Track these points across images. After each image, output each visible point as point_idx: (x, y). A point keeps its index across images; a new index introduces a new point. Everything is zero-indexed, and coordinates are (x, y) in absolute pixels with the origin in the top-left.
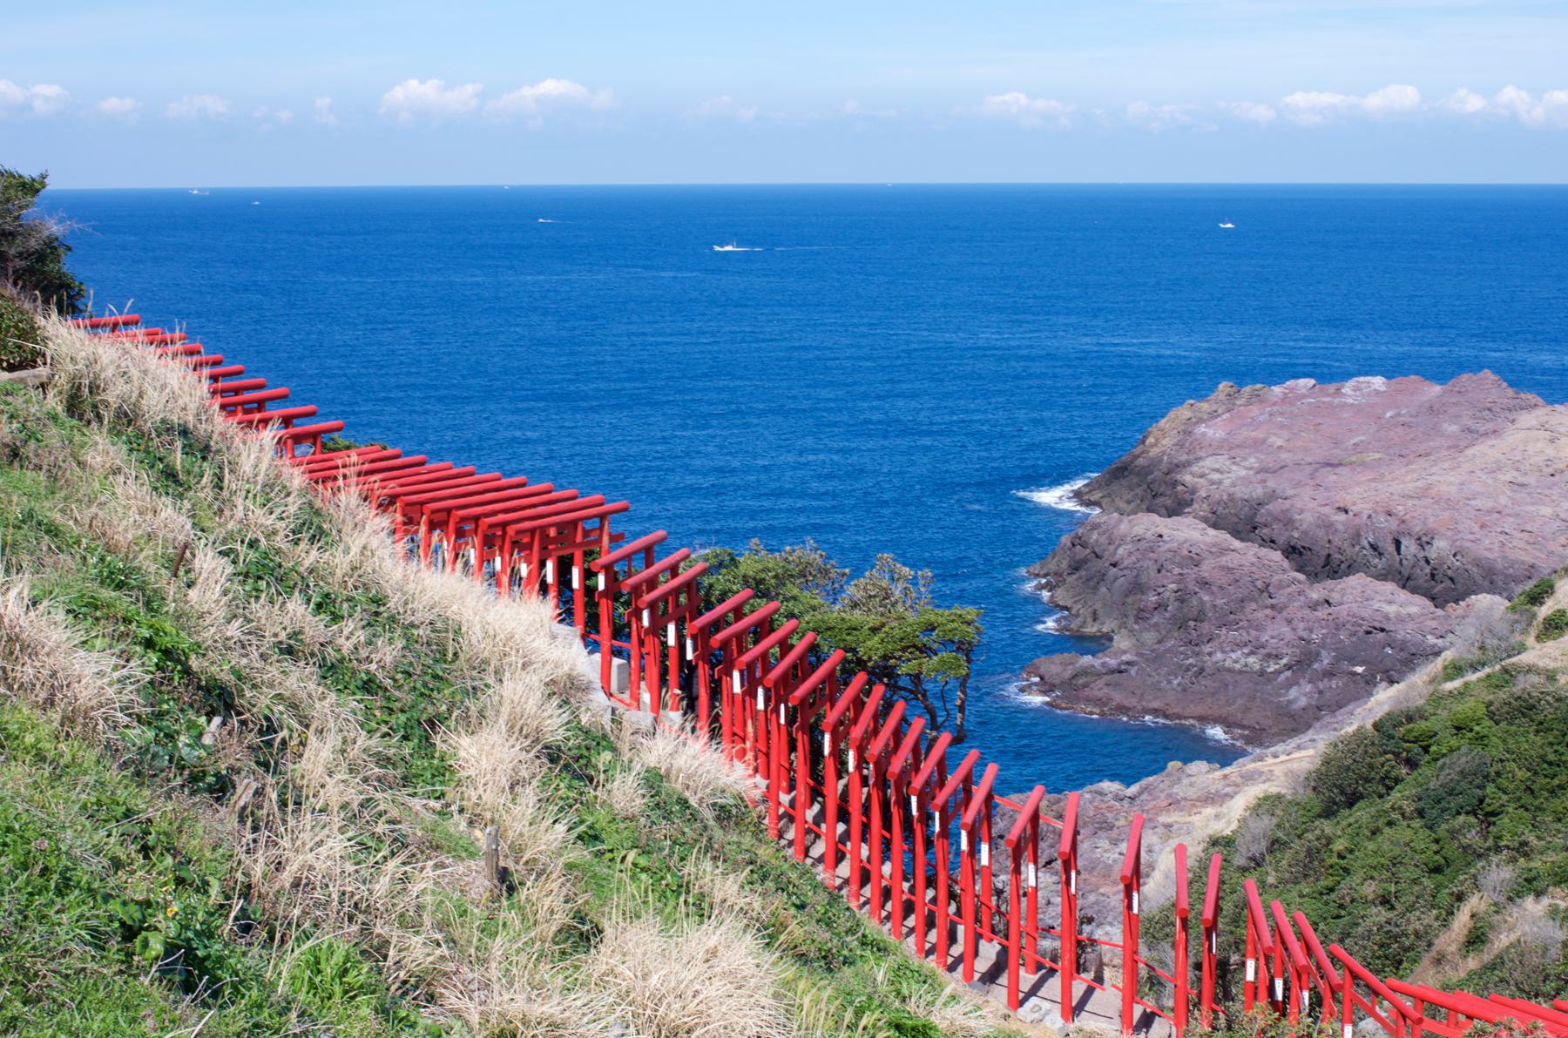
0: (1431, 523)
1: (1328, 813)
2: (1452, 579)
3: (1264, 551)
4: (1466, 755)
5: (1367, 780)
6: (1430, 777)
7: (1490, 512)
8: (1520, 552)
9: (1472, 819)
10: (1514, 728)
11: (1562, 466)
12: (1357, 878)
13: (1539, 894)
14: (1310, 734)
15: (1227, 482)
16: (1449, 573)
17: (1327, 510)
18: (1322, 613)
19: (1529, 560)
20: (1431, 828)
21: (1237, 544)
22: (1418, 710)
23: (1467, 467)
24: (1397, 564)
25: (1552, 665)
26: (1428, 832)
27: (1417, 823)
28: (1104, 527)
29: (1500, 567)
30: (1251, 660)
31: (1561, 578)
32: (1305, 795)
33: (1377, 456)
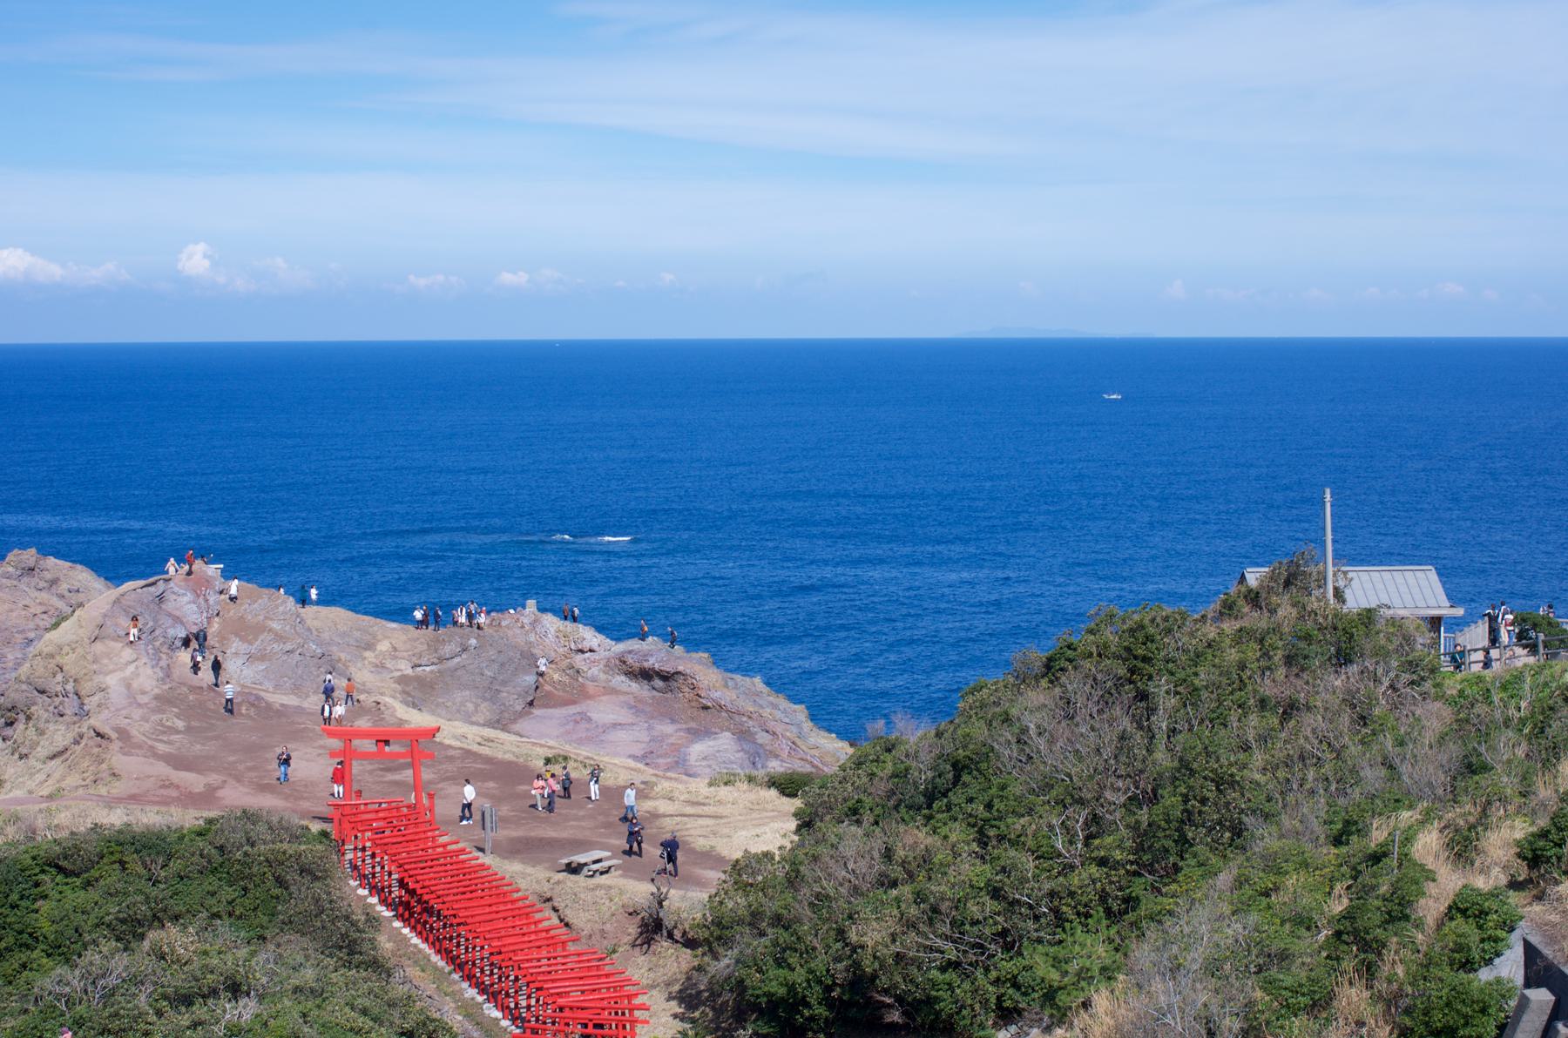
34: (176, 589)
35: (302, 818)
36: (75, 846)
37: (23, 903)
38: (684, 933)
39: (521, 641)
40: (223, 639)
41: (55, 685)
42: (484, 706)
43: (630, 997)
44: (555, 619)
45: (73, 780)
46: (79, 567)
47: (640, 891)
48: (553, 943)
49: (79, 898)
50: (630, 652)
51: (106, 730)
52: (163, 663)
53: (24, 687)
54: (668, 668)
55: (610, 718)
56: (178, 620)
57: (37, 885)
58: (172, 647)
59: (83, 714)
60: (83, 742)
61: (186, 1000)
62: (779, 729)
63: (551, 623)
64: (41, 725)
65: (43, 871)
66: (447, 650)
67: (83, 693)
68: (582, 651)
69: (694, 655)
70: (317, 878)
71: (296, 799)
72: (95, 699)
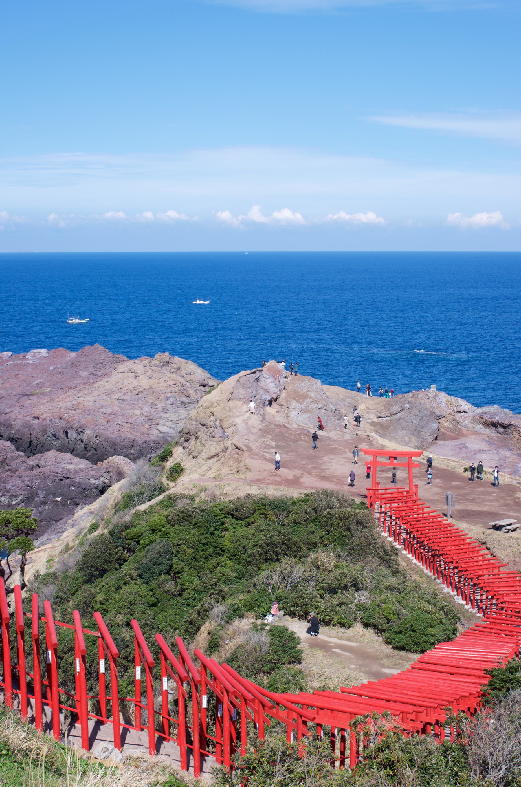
1: (88, 581)
2: (95, 449)
4: (160, 544)
5: (110, 562)
6: (142, 557)
7: (110, 414)
8: (128, 434)
9: (167, 577)
10: (182, 528)
11: (142, 390)
12: (112, 614)
13: (241, 617)
14: (46, 537)
16: (94, 446)
17: (28, 418)
18: (36, 472)
20: (147, 583)
22: (130, 522)
24: (67, 444)
25: (191, 493)
27: (139, 581)
29: (118, 441)
32: (72, 572)
33: (49, 389)
34: (265, 375)
36: (242, 505)
37: (216, 532)
39: (428, 406)
41: (210, 422)
42: (414, 439)
45: (225, 470)
46: (190, 362)
48: (492, 566)
50: (485, 413)
51: (240, 445)
52: (262, 412)
53: (194, 422)
54: (506, 422)
56: (266, 391)
57: (223, 523)
58: (264, 405)
59: (224, 437)
60: (228, 452)
61: (333, 591)
63: (443, 397)
64: (203, 442)
65: (225, 517)
66: (395, 409)
67: (224, 426)
68: (459, 412)
70: (365, 527)
71: (341, 484)
72: (231, 430)
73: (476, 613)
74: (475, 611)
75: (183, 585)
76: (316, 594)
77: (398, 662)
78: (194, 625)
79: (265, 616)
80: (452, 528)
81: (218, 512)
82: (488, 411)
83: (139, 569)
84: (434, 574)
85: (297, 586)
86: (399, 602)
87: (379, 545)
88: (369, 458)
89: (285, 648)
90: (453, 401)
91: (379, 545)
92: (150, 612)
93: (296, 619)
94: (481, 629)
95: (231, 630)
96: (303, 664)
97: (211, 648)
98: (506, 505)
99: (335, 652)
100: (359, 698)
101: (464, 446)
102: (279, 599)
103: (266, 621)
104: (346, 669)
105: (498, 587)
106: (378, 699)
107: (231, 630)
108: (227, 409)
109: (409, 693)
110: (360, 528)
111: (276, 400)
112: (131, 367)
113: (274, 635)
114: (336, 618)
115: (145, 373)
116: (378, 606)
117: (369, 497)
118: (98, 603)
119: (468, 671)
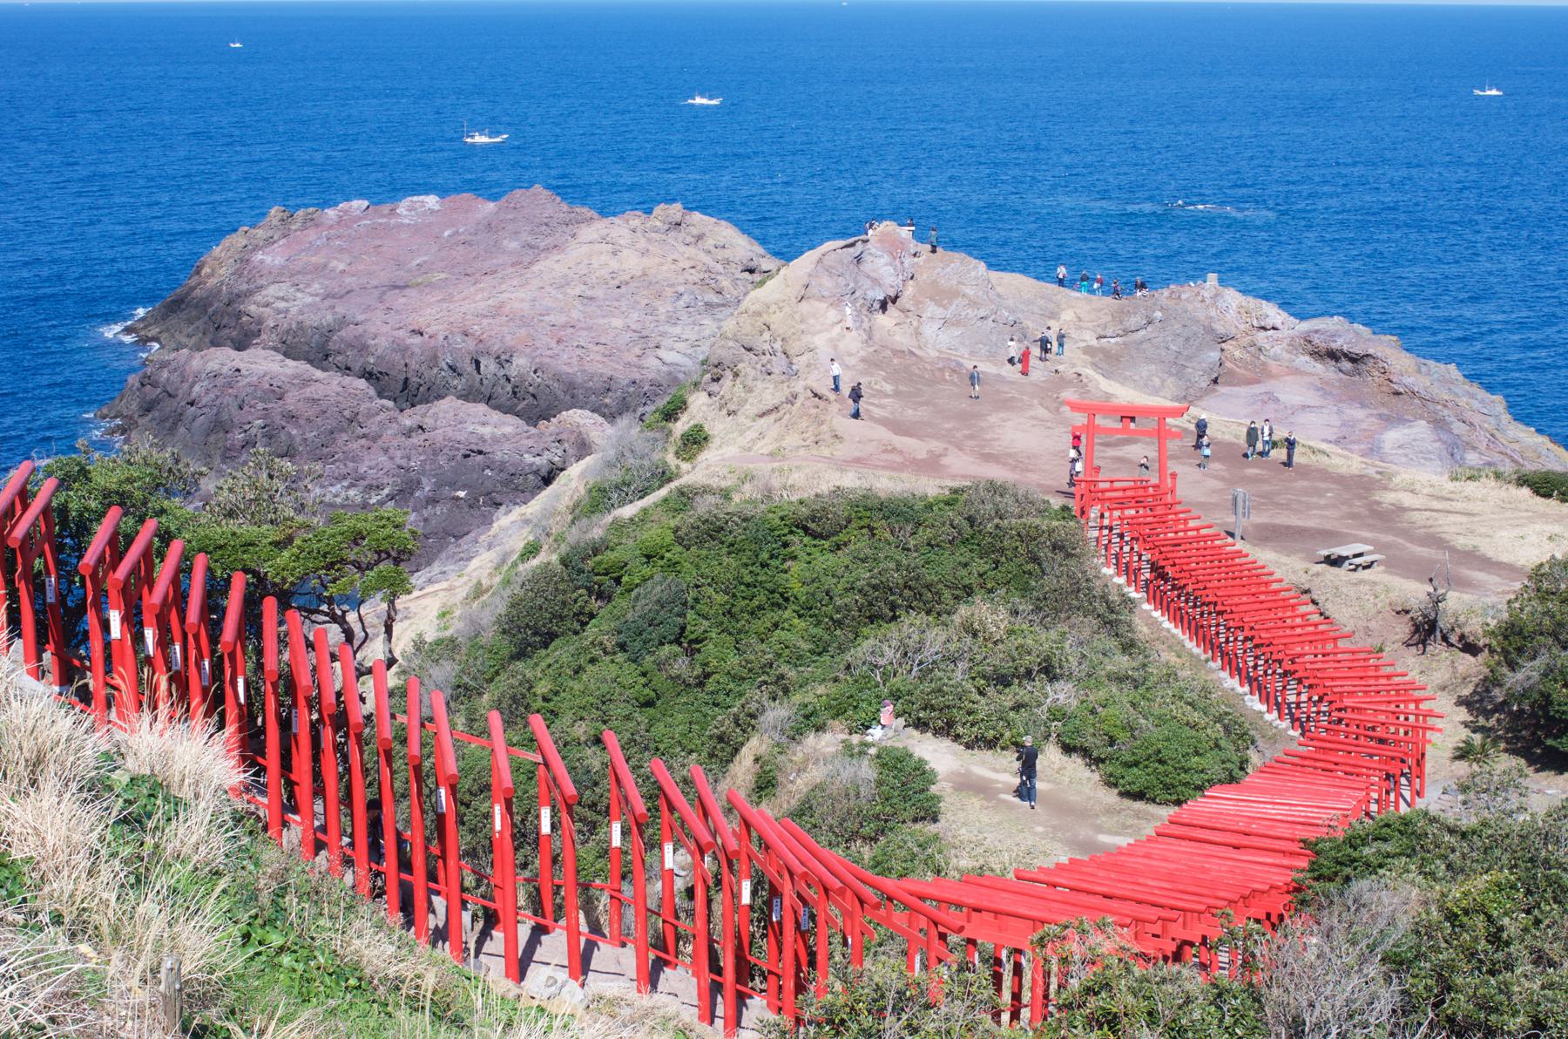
0: (510, 341)
1: (520, 655)
2: (534, 396)
3: (348, 380)
5: (562, 618)
7: (564, 327)
8: (598, 366)
9: (676, 648)
10: (704, 552)
11: (627, 277)
12: (567, 719)
13: (820, 728)
14: (436, 568)
15: (294, 310)
16: (531, 389)
17: (401, 333)
18: (417, 439)
19: (610, 373)
20: (634, 661)
21: (319, 374)
23: (536, 283)
24: (477, 384)
25: (724, 484)
26: (634, 666)
27: (620, 657)
28: (174, 365)
29: (579, 379)
30: (352, 493)
31: (691, 392)
32: (489, 636)
33: (443, 276)
35: (1047, 492)
37: (773, 563)
38: (1462, 637)
39: (1201, 315)
40: (917, 303)
41: (762, 343)
42: (1170, 381)
43: (1417, 701)
44: (1238, 294)
45: (792, 440)
46: (723, 223)
47: (1415, 592)
48: (1324, 638)
49: (826, 560)
50: (1316, 332)
52: (866, 325)
53: (731, 344)
54: (1358, 350)
55: (1297, 399)
56: (876, 282)
57: (785, 545)
58: (870, 310)
59: (791, 374)
60: (798, 404)
61: (1003, 681)
62: (1477, 419)
63: (1232, 298)
64: (749, 382)
65: (791, 532)
66: (1134, 321)
67: (791, 352)
68: (1264, 328)
69: (1383, 337)
70: (1069, 555)
72: (804, 359)
73: (1286, 730)
74: (1285, 724)
75: (707, 664)
76: (969, 686)
77: (1130, 822)
78: (727, 743)
79: (868, 727)
80: (1243, 560)
81: (778, 521)
82: (1321, 327)
83: (619, 632)
84: (1205, 652)
85: (932, 670)
86: (1133, 705)
87: (1097, 592)
88: (1080, 419)
89: (908, 792)
90: (1252, 305)
91: (1097, 592)
92: (641, 717)
93: (929, 734)
94: (1296, 760)
95: (800, 755)
96: (942, 824)
97: (761, 788)
98: (1354, 516)
99: (1005, 801)
100: (1051, 890)
101: (1271, 398)
102: (896, 696)
103: (869, 739)
104: (1027, 835)
105: (1333, 679)
106: (1089, 892)
107: (800, 755)
108: (797, 317)
109: (1151, 883)
110: (1059, 556)
111: (894, 300)
112: (605, 232)
113: (884, 765)
114: (1008, 734)
115: (633, 244)
116: (1093, 712)
117: (1078, 497)
118: (540, 699)
119: (1267, 843)
